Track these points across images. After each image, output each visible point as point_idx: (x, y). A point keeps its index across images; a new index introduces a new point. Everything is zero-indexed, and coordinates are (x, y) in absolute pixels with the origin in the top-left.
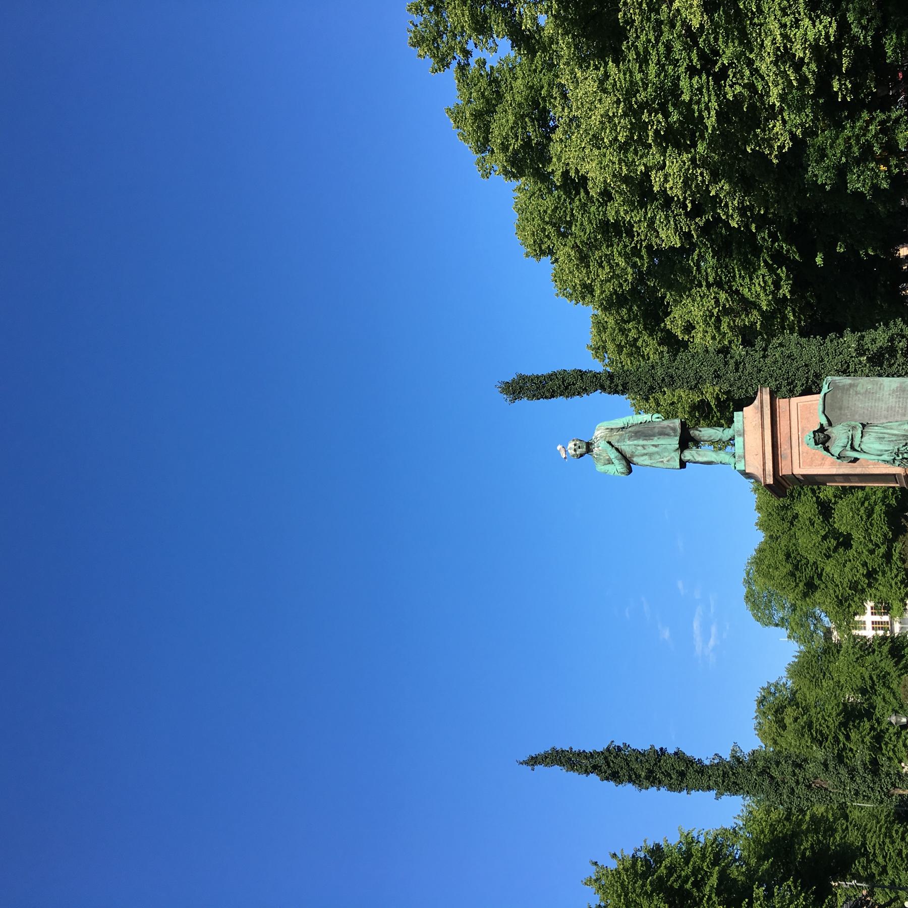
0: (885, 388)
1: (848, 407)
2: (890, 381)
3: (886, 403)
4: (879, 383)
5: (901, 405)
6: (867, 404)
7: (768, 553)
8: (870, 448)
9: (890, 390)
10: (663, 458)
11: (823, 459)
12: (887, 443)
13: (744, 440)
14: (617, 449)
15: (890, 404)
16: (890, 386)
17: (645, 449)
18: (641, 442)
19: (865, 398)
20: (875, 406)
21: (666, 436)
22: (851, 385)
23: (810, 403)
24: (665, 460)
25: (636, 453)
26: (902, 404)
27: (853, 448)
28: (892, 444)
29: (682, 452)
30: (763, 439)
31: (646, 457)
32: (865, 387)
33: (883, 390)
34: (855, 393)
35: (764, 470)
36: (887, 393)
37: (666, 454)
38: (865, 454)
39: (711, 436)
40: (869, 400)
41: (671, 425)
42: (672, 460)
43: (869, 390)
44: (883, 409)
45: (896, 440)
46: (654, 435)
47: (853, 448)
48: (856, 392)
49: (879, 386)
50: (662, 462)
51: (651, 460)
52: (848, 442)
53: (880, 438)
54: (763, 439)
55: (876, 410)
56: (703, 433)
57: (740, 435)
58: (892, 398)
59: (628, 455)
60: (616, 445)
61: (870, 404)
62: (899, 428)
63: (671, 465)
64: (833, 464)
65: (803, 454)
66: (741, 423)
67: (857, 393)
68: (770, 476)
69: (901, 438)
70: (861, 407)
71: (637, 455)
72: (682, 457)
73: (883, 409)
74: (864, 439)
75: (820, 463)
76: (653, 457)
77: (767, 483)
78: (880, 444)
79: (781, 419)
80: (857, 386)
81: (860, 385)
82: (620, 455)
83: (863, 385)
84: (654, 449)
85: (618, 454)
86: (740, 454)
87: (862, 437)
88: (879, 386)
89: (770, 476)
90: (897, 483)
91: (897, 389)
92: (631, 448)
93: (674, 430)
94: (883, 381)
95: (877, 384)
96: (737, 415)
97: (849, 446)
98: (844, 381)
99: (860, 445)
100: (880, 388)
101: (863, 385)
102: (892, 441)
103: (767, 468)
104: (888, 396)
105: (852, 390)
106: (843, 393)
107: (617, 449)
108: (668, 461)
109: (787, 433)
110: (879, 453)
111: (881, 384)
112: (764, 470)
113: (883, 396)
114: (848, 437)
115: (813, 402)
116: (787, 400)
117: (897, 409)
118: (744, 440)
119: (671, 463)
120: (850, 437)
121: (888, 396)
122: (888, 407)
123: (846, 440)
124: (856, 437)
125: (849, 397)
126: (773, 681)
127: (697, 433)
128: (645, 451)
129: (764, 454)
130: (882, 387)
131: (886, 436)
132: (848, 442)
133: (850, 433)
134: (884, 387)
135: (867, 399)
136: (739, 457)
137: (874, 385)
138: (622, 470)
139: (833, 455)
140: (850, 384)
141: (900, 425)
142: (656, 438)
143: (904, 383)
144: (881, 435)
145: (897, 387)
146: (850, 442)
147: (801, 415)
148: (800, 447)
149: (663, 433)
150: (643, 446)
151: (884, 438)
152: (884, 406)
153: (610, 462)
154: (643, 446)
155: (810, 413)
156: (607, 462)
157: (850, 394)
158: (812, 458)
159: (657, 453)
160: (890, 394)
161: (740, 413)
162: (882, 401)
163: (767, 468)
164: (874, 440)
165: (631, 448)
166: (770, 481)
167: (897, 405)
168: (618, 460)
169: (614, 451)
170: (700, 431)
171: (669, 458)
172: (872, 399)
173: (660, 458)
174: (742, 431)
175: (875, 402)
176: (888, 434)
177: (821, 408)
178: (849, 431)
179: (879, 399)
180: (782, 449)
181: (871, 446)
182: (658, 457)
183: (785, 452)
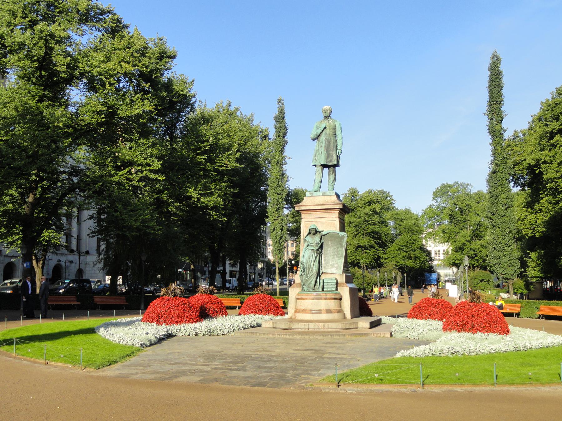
14: (321, 133)
18: (324, 145)
21: (326, 158)
22: (341, 245)
27: (308, 246)
41: (333, 160)
47: (308, 246)
59: (319, 138)
60: (324, 132)
66: (329, 194)
67: (338, 248)
74: (310, 251)
81: (341, 249)
82: (318, 134)
84: (320, 152)
93: (331, 161)
107: (321, 133)
126: (393, 198)
129: (313, 205)
131: (311, 260)
133: (314, 245)
142: (325, 152)
144: (311, 258)
149: (328, 156)
150: (322, 146)
154: (322, 146)
169: (320, 131)
181: (307, 253)
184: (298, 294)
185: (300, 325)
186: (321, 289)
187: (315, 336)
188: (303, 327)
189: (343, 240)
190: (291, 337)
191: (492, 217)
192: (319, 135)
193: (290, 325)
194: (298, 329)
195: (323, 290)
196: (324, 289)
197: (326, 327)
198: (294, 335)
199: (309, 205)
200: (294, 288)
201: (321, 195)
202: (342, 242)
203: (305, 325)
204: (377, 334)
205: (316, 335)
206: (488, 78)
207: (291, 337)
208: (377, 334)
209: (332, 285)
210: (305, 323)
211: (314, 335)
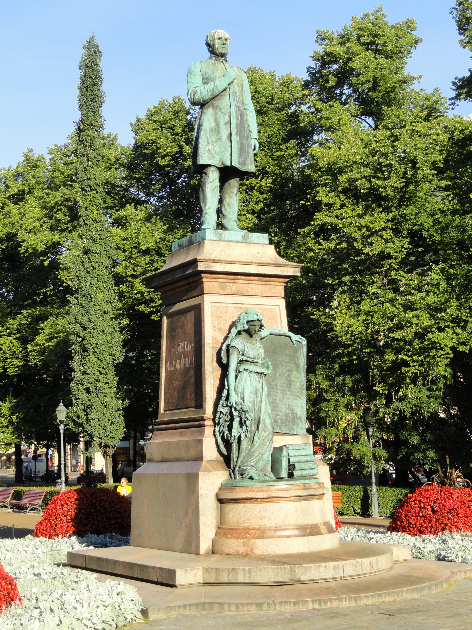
0: (295, 401)
2: (302, 406)
3: (280, 401)
4: (300, 395)
7: (275, 239)
8: (245, 381)
10: (212, 144)
11: (220, 329)
12: (252, 399)
13: (239, 242)
16: (297, 406)
17: (226, 124)
20: (277, 390)
22: (298, 365)
23: (279, 320)
24: (210, 147)
25: (219, 113)
28: (251, 405)
29: (218, 168)
30: (247, 263)
31: (213, 125)
33: (294, 399)
34: (290, 368)
35: (214, 261)
36: (290, 403)
37: (217, 149)
38: (234, 377)
39: (229, 205)
41: (249, 161)
42: (211, 156)
46: (240, 138)
49: (298, 394)
50: (208, 143)
51: (210, 130)
52: (249, 358)
53: (257, 392)
54: (247, 263)
56: (234, 197)
57: (244, 239)
59: (216, 103)
62: (267, 414)
63: (205, 153)
64: (214, 340)
65: (226, 307)
66: (257, 241)
67: (290, 371)
68: (207, 267)
71: (215, 115)
72: (212, 169)
74: (254, 376)
75: (216, 326)
76: (213, 133)
77: (199, 263)
78: (251, 392)
79: (263, 286)
80: (297, 371)
81: (298, 375)
82: (218, 93)
83: (298, 378)
85: (220, 90)
86: (223, 236)
87: (257, 373)
88: (298, 394)
89: (207, 267)
90: (165, 411)
92: (226, 107)
93: (244, 163)
94: (303, 399)
95: (299, 393)
96: (264, 237)
97: (245, 358)
98: (303, 358)
100: (295, 396)
101: (298, 378)
102: (254, 405)
103: (215, 264)
104: (287, 403)
105: (293, 365)
108: (209, 151)
109: (248, 291)
110: (240, 391)
111: (299, 397)
112: (214, 261)
113: (288, 398)
114: (255, 358)
115: (279, 324)
116: (283, 295)
118: (239, 242)
119: (207, 154)
120: (256, 360)
121: (287, 403)
123: (252, 356)
124: (256, 367)
125: (286, 362)
127: (235, 190)
128: (222, 124)
129: (226, 262)
131: (259, 399)
132: (249, 358)
133: (259, 360)
136: (220, 235)
138: (198, 93)
141: (269, 413)
142: (238, 139)
143: (301, 420)
144: (259, 394)
145: (297, 414)
146: (250, 360)
147: (266, 309)
148: (232, 305)
151: (256, 397)
153: (206, 81)
155: (269, 319)
156: (206, 76)
157: (289, 363)
158: (221, 317)
159: (219, 139)
160: (289, 406)
161: (267, 241)
163: (215, 264)
165: (226, 107)
166: (201, 267)
168: (213, 89)
170: (236, 195)
171: (213, 153)
172: (284, 387)
173: (212, 142)
174: (248, 241)
175: (281, 390)
176: (216, 405)
177: (276, 332)
180: (231, 285)
182: (214, 139)
183: (228, 287)
184: (223, 487)
185: (322, 569)
186: (284, 474)
187: (404, 595)
188: (330, 574)
189: (299, 354)
190: (353, 604)
191: (82, 334)
192: (217, 95)
193: (293, 571)
194: (316, 581)
195: (291, 475)
196: (296, 473)
197: (367, 570)
198: (360, 598)
199: (226, 262)
200: (211, 473)
201: (240, 239)
202: (298, 358)
203: (335, 567)
204: (465, 572)
205: (407, 592)
206: (79, 82)
207: (353, 604)
208: (465, 572)
209: (307, 461)
210: (336, 563)
211: (402, 592)
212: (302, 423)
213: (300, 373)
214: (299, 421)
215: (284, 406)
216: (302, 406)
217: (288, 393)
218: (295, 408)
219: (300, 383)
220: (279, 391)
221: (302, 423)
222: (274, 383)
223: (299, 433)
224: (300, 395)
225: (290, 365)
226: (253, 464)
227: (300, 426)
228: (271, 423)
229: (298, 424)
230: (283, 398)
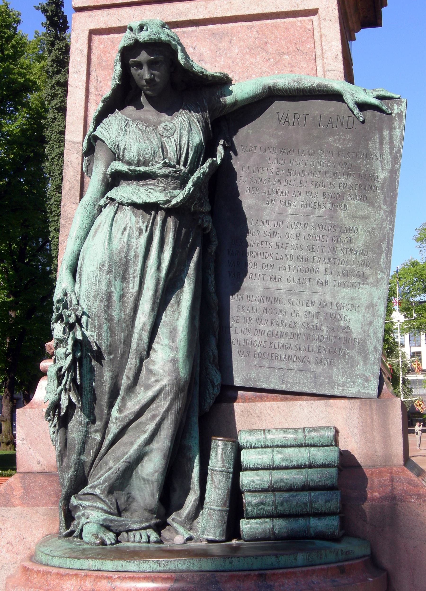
0: (345, 291)
1: (289, 172)
3: (290, 292)
4: (368, 271)
5: (283, 341)
6: (293, 231)
9: (339, 306)
15: (287, 307)
16: (354, 307)
19: (318, 226)
26: (284, 346)
32: (359, 225)
33: (342, 285)
34: (338, 191)
36: (328, 298)
40: (309, 238)
43: (344, 236)
44: (272, 285)
45: (110, 319)
48: (342, 196)
52: (129, 163)
55: (267, 261)
58: (307, 313)
61: (294, 242)
69: (121, 336)
70: (284, 213)
73: (272, 285)
80: (363, 198)
81: (366, 208)
83: (365, 218)
87: (135, 205)
88: (358, 269)
91: (342, 328)
94: (376, 284)
95: (363, 264)
99: (112, 200)
100: (347, 274)
101: (365, 218)
104: (316, 298)
105: (350, 182)
106: (342, 152)
111: (364, 277)
114: (146, 164)
117: (267, 329)
120: (142, 169)
121: (316, 298)
122: (277, 300)
130: (354, 280)
132: (129, 163)
134: (352, 286)
135: (311, 231)
137: (364, 253)
139: (98, 120)
140: (374, 177)
143: (364, 352)
145: (348, 330)
146: (124, 168)
151: (124, 279)
152: (283, 285)
155: (281, 54)
157: (335, 175)
160: (323, 305)
162: (301, 282)
164: (117, 244)
167: (280, 329)
178: (166, 165)
179: (307, 270)
202: (369, 156)
212: (366, 358)
213: (371, 204)
214: (354, 353)
215: (302, 309)
216: (371, 306)
217: (322, 267)
218: (343, 312)
219: (371, 232)
220: (289, 263)
221: (366, 358)
222: (275, 240)
223: (352, 391)
224: (368, 271)
225: (341, 180)
226: (98, 491)
227: (360, 370)
228: (174, 361)
229: (352, 364)
230: (301, 282)
